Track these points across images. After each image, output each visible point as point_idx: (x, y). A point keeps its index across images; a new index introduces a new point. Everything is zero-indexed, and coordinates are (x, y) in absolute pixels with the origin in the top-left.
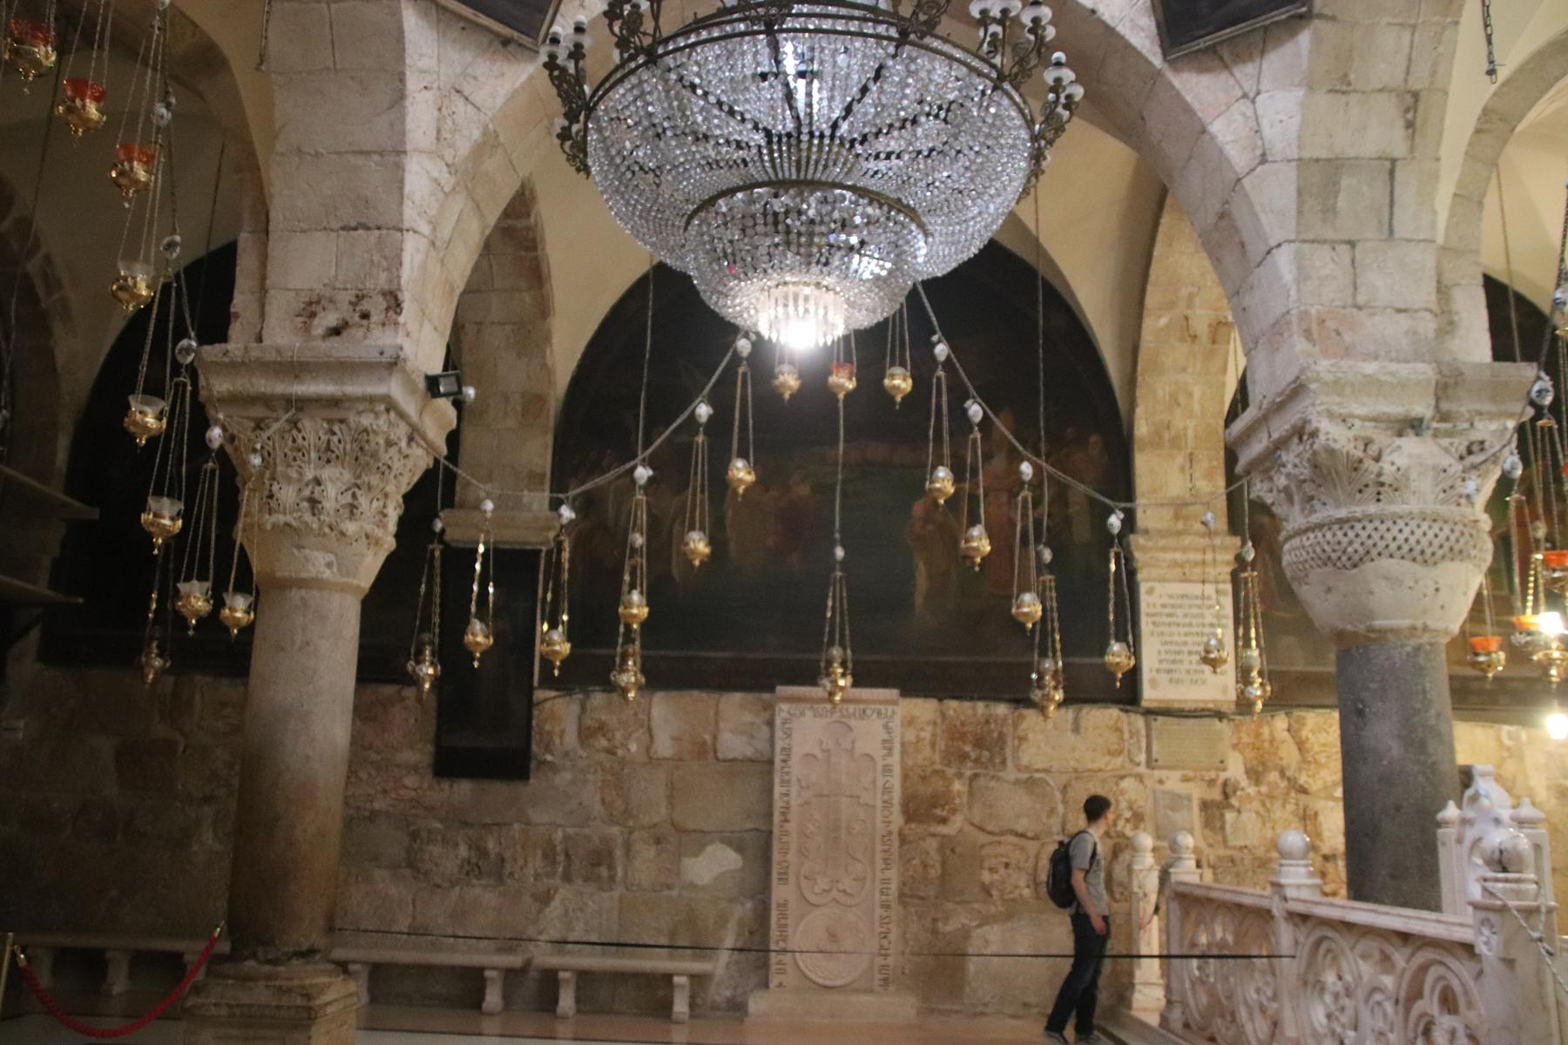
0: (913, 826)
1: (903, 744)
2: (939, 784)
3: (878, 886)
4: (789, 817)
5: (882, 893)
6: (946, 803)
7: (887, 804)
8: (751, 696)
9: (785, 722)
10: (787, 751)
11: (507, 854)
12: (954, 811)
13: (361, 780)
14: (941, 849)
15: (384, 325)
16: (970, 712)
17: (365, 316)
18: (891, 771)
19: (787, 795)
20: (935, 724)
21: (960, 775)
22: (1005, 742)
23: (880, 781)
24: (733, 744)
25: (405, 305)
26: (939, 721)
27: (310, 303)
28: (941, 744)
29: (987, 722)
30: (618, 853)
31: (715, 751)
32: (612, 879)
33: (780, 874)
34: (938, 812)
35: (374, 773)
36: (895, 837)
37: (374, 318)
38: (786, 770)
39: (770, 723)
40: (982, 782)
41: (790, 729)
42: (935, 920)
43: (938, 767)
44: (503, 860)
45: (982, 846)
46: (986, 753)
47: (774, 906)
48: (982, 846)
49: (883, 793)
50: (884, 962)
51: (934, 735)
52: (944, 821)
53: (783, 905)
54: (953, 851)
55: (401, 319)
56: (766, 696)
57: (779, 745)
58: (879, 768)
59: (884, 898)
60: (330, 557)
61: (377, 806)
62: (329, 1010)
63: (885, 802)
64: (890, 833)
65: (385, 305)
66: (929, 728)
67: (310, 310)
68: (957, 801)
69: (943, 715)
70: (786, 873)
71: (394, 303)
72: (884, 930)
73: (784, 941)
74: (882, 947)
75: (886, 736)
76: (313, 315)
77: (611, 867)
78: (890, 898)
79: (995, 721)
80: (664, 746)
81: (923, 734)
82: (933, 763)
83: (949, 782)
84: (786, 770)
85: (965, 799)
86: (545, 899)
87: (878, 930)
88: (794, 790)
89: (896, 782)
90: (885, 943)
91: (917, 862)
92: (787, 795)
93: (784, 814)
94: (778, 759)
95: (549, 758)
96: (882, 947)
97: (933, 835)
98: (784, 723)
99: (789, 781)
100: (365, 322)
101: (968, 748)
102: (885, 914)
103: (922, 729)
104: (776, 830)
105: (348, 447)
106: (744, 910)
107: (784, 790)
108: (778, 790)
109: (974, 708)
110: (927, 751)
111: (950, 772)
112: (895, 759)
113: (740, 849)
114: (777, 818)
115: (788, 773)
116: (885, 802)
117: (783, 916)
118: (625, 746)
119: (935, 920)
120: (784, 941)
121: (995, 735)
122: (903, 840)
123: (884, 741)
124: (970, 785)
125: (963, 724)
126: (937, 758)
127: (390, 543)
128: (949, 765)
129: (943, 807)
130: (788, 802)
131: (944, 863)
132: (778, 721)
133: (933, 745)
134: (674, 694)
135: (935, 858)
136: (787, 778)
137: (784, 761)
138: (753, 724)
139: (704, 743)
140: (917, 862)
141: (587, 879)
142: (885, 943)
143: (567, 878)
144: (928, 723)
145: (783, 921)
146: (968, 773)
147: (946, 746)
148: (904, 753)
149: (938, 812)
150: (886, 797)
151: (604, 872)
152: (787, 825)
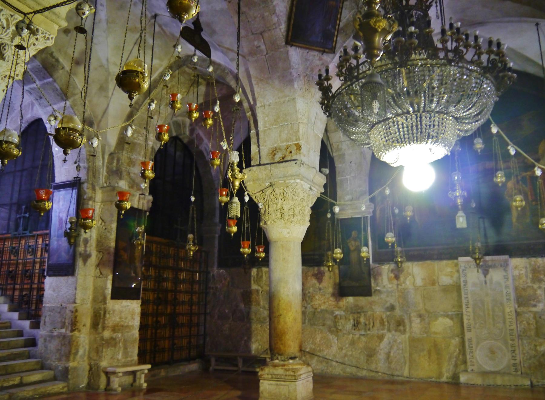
0: (522, 308)
1: (513, 276)
2: (530, 292)
3: (508, 332)
4: (469, 306)
5: (511, 335)
6: (535, 299)
7: (509, 300)
8: (450, 262)
9: (463, 271)
10: (466, 282)
11: (367, 323)
12: (539, 302)
13: (316, 299)
14: (535, 318)
15: (296, 154)
16: (541, 262)
17: (291, 152)
19: (467, 298)
20: (526, 268)
21: (540, 288)
23: (505, 292)
24: (445, 280)
25: (302, 147)
26: (528, 266)
27: (274, 151)
28: (530, 276)
30: (407, 321)
31: (438, 283)
32: (405, 331)
34: (532, 302)
35: (320, 297)
36: (514, 313)
37: (293, 153)
38: (466, 288)
39: (458, 271)
41: (466, 273)
42: (536, 346)
43: (530, 284)
44: (366, 325)
49: (506, 296)
51: (526, 272)
52: (535, 306)
53: (470, 340)
54: (540, 317)
55: (302, 151)
56: (455, 261)
57: (462, 279)
59: (511, 337)
60: (288, 231)
61: (322, 307)
62: (302, 377)
63: (507, 299)
65: (296, 148)
67: (274, 152)
68: (540, 298)
69: (530, 264)
71: (299, 147)
72: (513, 349)
73: (472, 353)
74: (513, 357)
75: (505, 274)
76: (275, 155)
77: (404, 326)
78: (514, 337)
80: (419, 282)
81: (522, 272)
83: (535, 291)
84: (466, 288)
86: (381, 338)
87: (511, 349)
88: (470, 296)
89: (511, 291)
90: (514, 354)
91: (525, 322)
93: (467, 305)
94: (462, 284)
95: (378, 288)
96: (513, 357)
97: (530, 312)
98: (463, 271)
99: (467, 293)
100: (290, 154)
103: (521, 270)
104: (464, 311)
105: (290, 194)
106: (456, 341)
107: (466, 296)
108: (463, 296)
110: (524, 278)
111: (536, 286)
112: (510, 282)
113: (452, 319)
114: (464, 306)
115: (467, 290)
116: (507, 299)
117: (470, 343)
118: (404, 282)
119: (536, 346)
120: (472, 353)
122: (518, 314)
123: (504, 276)
125: (539, 267)
126: (529, 281)
127: (308, 224)
128: (534, 283)
129: (534, 300)
130: (468, 301)
131: (537, 322)
132: (461, 271)
133: (527, 276)
134: (420, 263)
135: (532, 321)
136: (466, 291)
137: (465, 285)
139: (434, 280)
140: (525, 322)
141: (396, 331)
142: (514, 354)
143: (389, 330)
144: (524, 268)
145: (471, 346)
147: (533, 276)
148: (514, 279)
149: (532, 302)
150: (508, 297)
151: (401, 328)
152: (468, 310)
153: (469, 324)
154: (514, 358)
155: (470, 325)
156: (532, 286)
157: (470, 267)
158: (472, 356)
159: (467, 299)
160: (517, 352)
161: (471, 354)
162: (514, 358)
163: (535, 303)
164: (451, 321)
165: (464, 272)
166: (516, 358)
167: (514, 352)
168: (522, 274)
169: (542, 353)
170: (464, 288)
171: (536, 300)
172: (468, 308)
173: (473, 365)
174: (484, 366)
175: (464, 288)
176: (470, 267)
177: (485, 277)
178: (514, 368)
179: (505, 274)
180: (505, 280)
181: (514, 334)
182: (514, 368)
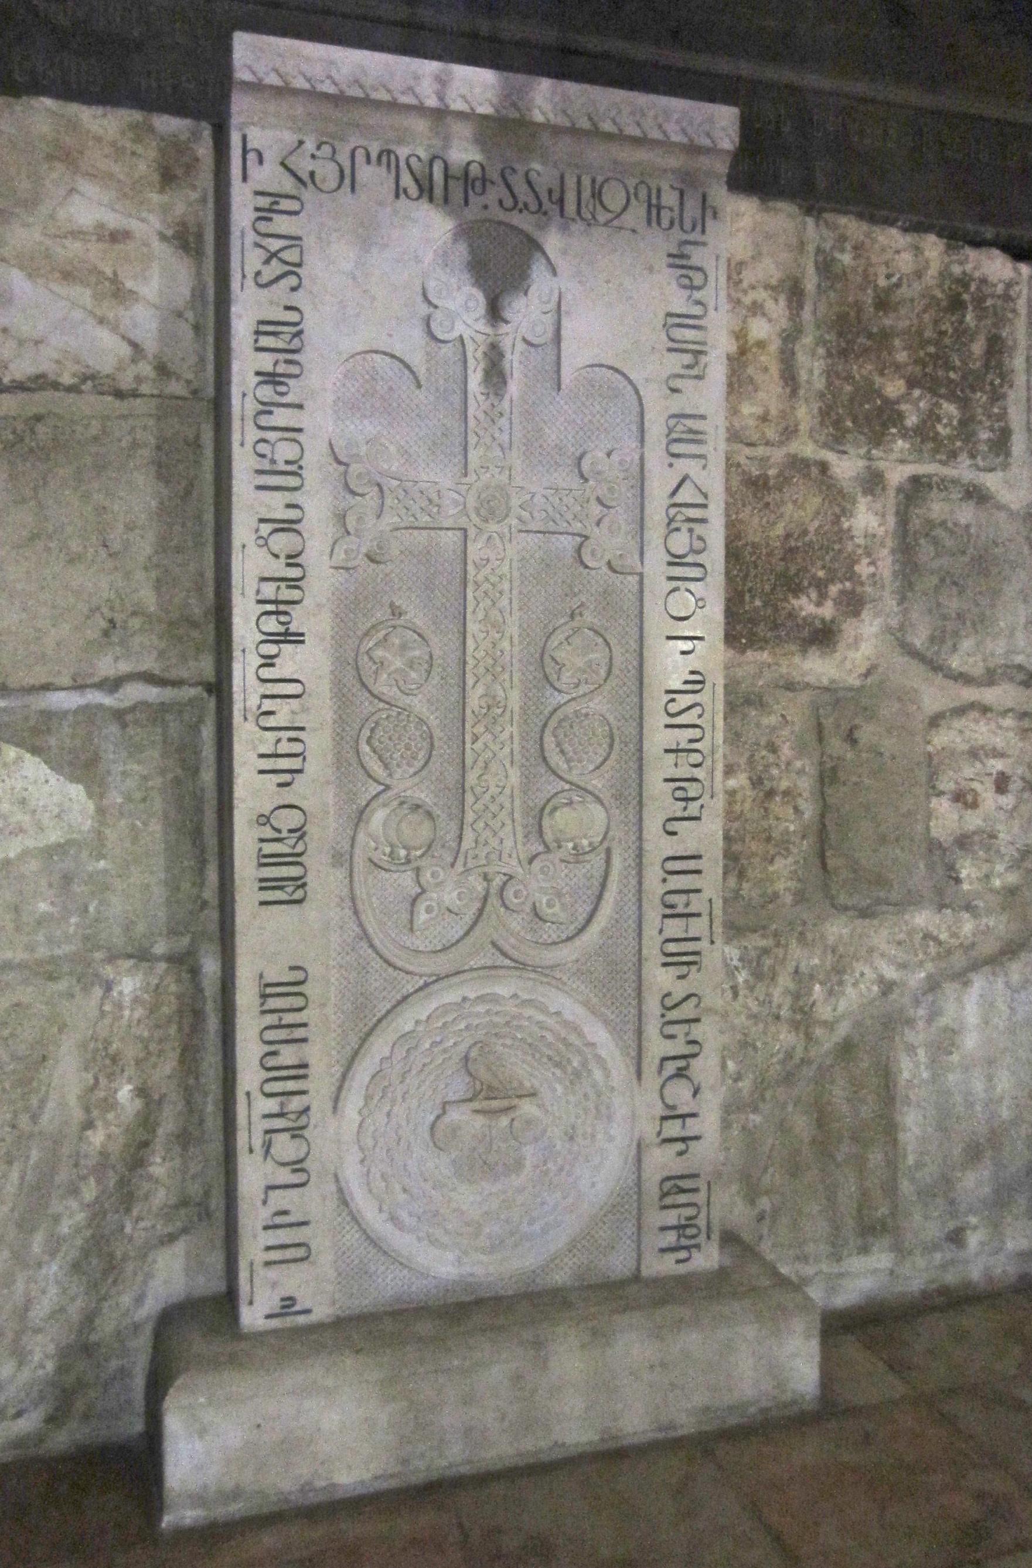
3: (654, 884)
18: (696, 437)
19: (287, 526)
20: (794, 292)
21: (873, 482)
22: (1005, 376)
26: (810, 283)
29: (956, 304)
33: (265, 860)
34: (806, 606)
38: (281, 417)
40: (937, 508)
43: (808, 450)
45: (935, 721)
46: (950, 409)
47: (246, 996)
48: (935, 721)
50: (678, 1167)
51: (790, 337)
54: (851, 738)
58: (656, 429)
59: (675, 929)
63: (676, 560)
64: (696, 682)
66: (778, 309)
68: (863, 569)
69: (826, 267)
70: (295, 859)
72: (678, 1047)
73: (296, 1133)
75: (679, 302)
79: (979, 301)
82: (789, 432)
84: (281, 417)
85: (886, 564)
87: (657, 1047)
90: (680, 1094)
92: (287, 526)
98: (264, 214)
99: (295, 466)
101: (894, 388)
102: (680, 990)
103: (756, 309)
107: (275, 505)
109: (917, 250)
116: (676, 560)
120: (296, 1133)
121: (978, 347)
123: (674, 320)
124: (903, 520)
125: (884, 303)
126: (805, 414)
128: (837, 441)
129: (821, 586)
130: (293, 559)
136: (285, 451)
137: (270, 378)
138: (117, 237)
142: (680, 1094)
145: (288, 1056)
146: (897, 475)
147: (830, 373)
149: (806, 606)
150: (680, 543)
153: (290, 820)
154: (673, 1129)
155: (299, 832)
156: (824, 467)
157: (348, 179)
158: (297, 1165)
159: (282, 542)
160: (705, 1068)
161: (285, 1147)
162: (673, 1129)
163: (827, 611)
164: (77, 791)
165: (282, 224)
166: (693, 1127)
167: (681, 1074)
168: (761, 344)
169: (843, 1029)
170: (266, 408)
171: (834, 589)
172: (289, 637)
173: (302, 1256)
174: (402, 1242)
175: (266, 408)
176: (348, 179)
177: (495, 313)
178: (671, 1217)
179: (679, 302)
180: (676, 362)
181: (697, 904)
182: (671, 1217)
